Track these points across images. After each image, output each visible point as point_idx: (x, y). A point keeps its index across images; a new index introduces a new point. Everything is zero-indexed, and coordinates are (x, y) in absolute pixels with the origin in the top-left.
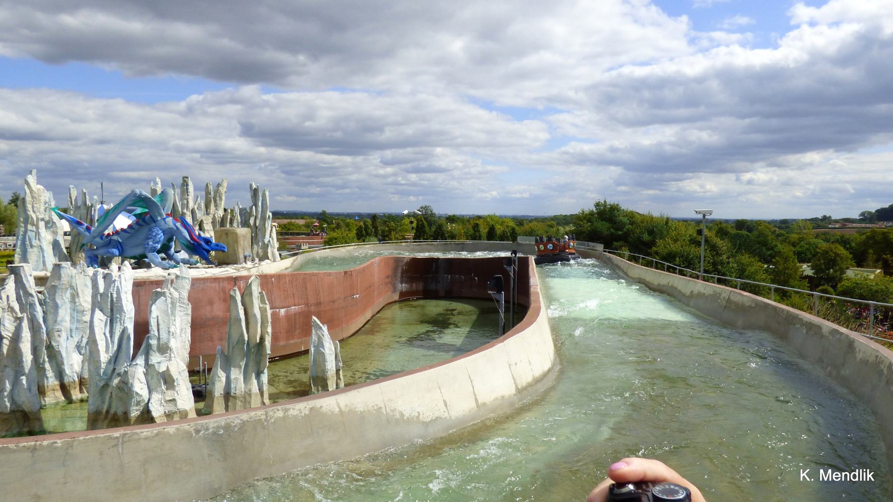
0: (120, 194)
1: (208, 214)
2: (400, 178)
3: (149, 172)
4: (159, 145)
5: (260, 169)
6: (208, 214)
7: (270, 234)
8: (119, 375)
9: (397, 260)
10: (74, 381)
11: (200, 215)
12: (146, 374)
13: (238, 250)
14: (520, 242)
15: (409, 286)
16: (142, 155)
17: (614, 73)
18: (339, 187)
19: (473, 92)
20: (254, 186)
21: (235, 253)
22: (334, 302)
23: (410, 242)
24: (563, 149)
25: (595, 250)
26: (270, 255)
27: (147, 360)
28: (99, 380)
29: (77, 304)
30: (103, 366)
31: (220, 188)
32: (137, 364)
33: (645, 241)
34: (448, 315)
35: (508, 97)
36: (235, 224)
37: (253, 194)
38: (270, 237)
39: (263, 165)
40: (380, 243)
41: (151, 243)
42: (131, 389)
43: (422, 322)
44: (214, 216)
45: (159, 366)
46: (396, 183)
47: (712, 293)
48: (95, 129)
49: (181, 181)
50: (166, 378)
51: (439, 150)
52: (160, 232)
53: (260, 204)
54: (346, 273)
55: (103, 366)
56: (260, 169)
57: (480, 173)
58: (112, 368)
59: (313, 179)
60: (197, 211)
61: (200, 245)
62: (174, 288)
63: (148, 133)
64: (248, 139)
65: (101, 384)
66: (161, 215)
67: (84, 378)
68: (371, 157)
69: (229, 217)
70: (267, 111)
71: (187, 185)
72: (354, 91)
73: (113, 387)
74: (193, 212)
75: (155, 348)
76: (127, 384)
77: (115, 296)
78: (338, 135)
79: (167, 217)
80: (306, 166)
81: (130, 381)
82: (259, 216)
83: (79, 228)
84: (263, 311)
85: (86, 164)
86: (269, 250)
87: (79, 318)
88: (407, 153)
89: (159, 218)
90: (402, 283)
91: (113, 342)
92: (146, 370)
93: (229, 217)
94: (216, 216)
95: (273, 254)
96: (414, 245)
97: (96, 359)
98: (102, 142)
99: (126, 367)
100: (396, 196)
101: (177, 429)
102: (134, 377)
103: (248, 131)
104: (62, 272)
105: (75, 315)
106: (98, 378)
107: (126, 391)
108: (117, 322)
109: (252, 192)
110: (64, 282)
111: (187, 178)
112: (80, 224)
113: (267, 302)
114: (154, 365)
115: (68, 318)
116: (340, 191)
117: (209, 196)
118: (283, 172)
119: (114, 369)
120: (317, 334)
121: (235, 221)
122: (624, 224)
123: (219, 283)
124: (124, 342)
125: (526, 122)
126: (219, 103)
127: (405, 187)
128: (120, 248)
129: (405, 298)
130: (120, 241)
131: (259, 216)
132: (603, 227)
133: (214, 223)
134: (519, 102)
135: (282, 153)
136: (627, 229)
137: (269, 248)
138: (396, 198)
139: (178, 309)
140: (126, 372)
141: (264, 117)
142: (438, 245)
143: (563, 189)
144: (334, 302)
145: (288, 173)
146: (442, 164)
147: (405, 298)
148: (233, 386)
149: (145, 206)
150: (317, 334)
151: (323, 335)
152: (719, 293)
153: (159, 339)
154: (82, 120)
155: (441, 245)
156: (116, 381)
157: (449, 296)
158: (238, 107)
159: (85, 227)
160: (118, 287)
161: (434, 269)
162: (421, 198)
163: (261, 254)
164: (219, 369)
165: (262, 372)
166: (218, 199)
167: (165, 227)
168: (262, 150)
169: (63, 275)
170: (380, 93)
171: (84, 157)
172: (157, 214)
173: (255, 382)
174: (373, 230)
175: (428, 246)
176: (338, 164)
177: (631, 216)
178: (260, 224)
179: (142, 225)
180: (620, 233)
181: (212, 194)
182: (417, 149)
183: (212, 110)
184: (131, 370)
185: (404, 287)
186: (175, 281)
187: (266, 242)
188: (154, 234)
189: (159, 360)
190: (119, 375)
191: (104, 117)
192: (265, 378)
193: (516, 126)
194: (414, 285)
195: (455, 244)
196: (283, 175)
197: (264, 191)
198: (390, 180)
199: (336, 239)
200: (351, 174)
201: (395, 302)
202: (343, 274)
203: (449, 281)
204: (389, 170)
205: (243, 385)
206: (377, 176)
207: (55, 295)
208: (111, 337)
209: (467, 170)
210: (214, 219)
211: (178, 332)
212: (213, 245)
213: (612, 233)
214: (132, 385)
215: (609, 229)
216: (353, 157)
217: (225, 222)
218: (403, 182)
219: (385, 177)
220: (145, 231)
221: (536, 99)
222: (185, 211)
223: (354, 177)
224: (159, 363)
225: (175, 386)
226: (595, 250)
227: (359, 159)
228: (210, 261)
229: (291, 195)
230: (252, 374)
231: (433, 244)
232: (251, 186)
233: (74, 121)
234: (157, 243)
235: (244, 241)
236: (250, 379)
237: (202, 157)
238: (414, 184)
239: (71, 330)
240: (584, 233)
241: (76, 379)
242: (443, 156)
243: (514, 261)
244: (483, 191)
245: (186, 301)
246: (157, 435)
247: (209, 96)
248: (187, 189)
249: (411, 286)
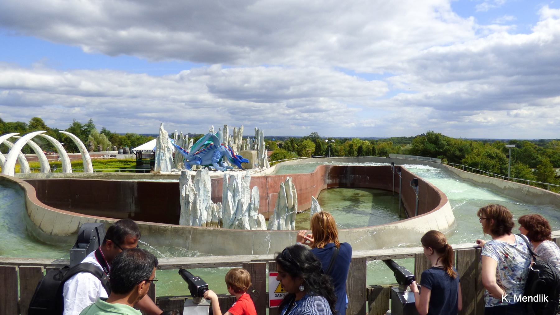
0: (141, 125)
1: (235, 143)
2: (297, 115)
3: (157, 114)
6: (235, 143)
7: (265, 153)
8: (238, 220)
9: (327, 167)
10: (205, 223)
11: (232, 144)
12: (249, 220)
13: (252, 162)
14: (391, 157)
15: (332, 181)
17: (425, 51)
18: (261, 121)
19: (342, 65)
20: (257, 129)
21: (251, 164)
22: (307, 189)
23: (329, 157)
24: (395, 97)
25: (436, 162)
26: (265, 164)
27: (249, 214)
28: (229, 222)
29: (206, 188)
30: (232, 216)
31: (240, 130)
32: (246, 216)
33: (457, 156)
34: (356, 196)
35: (363, 67)
36: (248, 149)
37: (256, 133)
38: (265, 155)
39: (218, 108)
40: (312, 158)
41: (215, 159)
42: (244, 227)
43: (345, 200)
44: (238, 144)
45: (254, 217)
46: (294, 119)
47: (518, 187)
48: (131, 90)
49: (223, 127)
50: (258, 222)
51: (321, 99)
52: (219, 153)
53: (260, 138)
54: (311, 174)
55: (232, 216)
56: (218, 111)
57: (345, 112)
58: (235, 217)
60: (231, 142)
61: (237, 159)
62: (244, 182)
65: (230, 224)
66: (219, 145)
67: (208, 222)
68: (282, 104)
69: (245, 145)
70: (223, 78)
71: (226, 129)
72: (274, 66)
73: (235, 225)
74: (229, 142)
75: (252, 208)
76: (241, 224)
77: (236, 185)
79: (222, 146)
80: (243, 109)
81: (244, 223)
83: (181, 151)
84: (294, 193)
87: (207, 195)
88: (302, 101)
89: (218, 146)
90: (328, 179)
91: (235, 206)
92: (249, 218)
93: (245, 145)
94: (239, 144)
95: (267, 164)
96: (331, 158)
97: (229, 213)
99: (241, 217)
100: (294, 126)
101: (362, 230)
102: (245, 221)
103: (213, 90)
104: (201, 174)
105: (205, 193)
106: (229, 221)
107: (241, 227)
108: (236, 197)
109: (256, 132)
110: (202, 178)
111: (226, 125)
112: (181, 149)
113: (295, 189)
114: (252, 216)
115: (203, 194)
116: (261, 124)
117: (236, 134)
119: (236, 217)
120: (314, 204)
121: (248, 147)
122: (444, 145)
123: (260, 179)
124: (240, 206)
125: (374, 81)
127: (300, 121)
128: (200, 161)
129: (330, 187)
130: (200, 157)
131: (259, 144)
132: (431, 147)
133: (238, 148)
134: (369, 70)
136: (446, 148)
137: (264, 160)
138: (293, 128)
139: (246, 191)
140: (241, 219)
142: (344, 158)
143: (395, 121)
144: (307, 189)
145: (232, 113)
146: (324, 107)
147: (330, 187)
148: (281, 227)
149: (212, 140)
150: (314, 204)
151: (317, 205)
152: (522, 188)
153: (254, 204)
154: (124, 85)
155: (346, 158)
156: (237, 223)
157: (352, 186)
159: (183, 150)
160: (237, 181)
161: (345, 171)
162: (309, 127)
163: (260, 164)
164: (275, 219)
165: (293, 221)
166: (239, 135)
167: (221, 151)
169: (202, 175)
172: (218, 144)
173: (290, 225)
174: (292, 148)
175: (340, 159)
176: (262, 108)
177: (449, 141)
178: (260, 148)
179: (210, 150)
180: (441, 150)
181: (237, 133)
182: (308, 99)
183: (194, 79)
184: (243, 218)
185: (329, 181)
186: (244, 178)
187: (263, 158)
188: (217, 154)
189: (254, 214)
190: (238, 220)
192: (294, 224)
193: (366, 84)
194: (334, 180)
195: (354, 158)
196: (230, 114)
197: (262, 131)
198: (291, 116)
199: (278, 154)
200: (269, 114)
201: (325, 189)
202: (310, 175)
203: (353, 178)
204: (292, 111)
205: (285, 227)
206: (284, 114)
207: (198, 184)
208: (234, 203)
209: (337, 111)
211: (245, 202)
212: (243, 160)
213: (436, 151)
214: (244, 224)
215: (434, 148)
216: (271, 104)
217: (243, 147)
218: (298, 118)
219: (288, 115)
220: (212, 153)
221: (379, 68)
222: (225, 142)
223: (270, 115)
224: (254, 215)
225: (261, 226)
226: (436, 162)
227: (274, 105)
228: (241, 168)
230: (289, 222)
231: (341, 158)
232: (255, 129)
233: (120, 86)
234: (218, 158)
235: (255, 157)
236: (288, 224)
238: (306, 119)
239: (204, 200)
240: (419, 150)
241: (206, 222)
242: (324, 103)
243: (393, 168)
244: (346, 123)
245: (249, 188)
246: (358, 231)
248: (226, 131)
249: (333, 181)
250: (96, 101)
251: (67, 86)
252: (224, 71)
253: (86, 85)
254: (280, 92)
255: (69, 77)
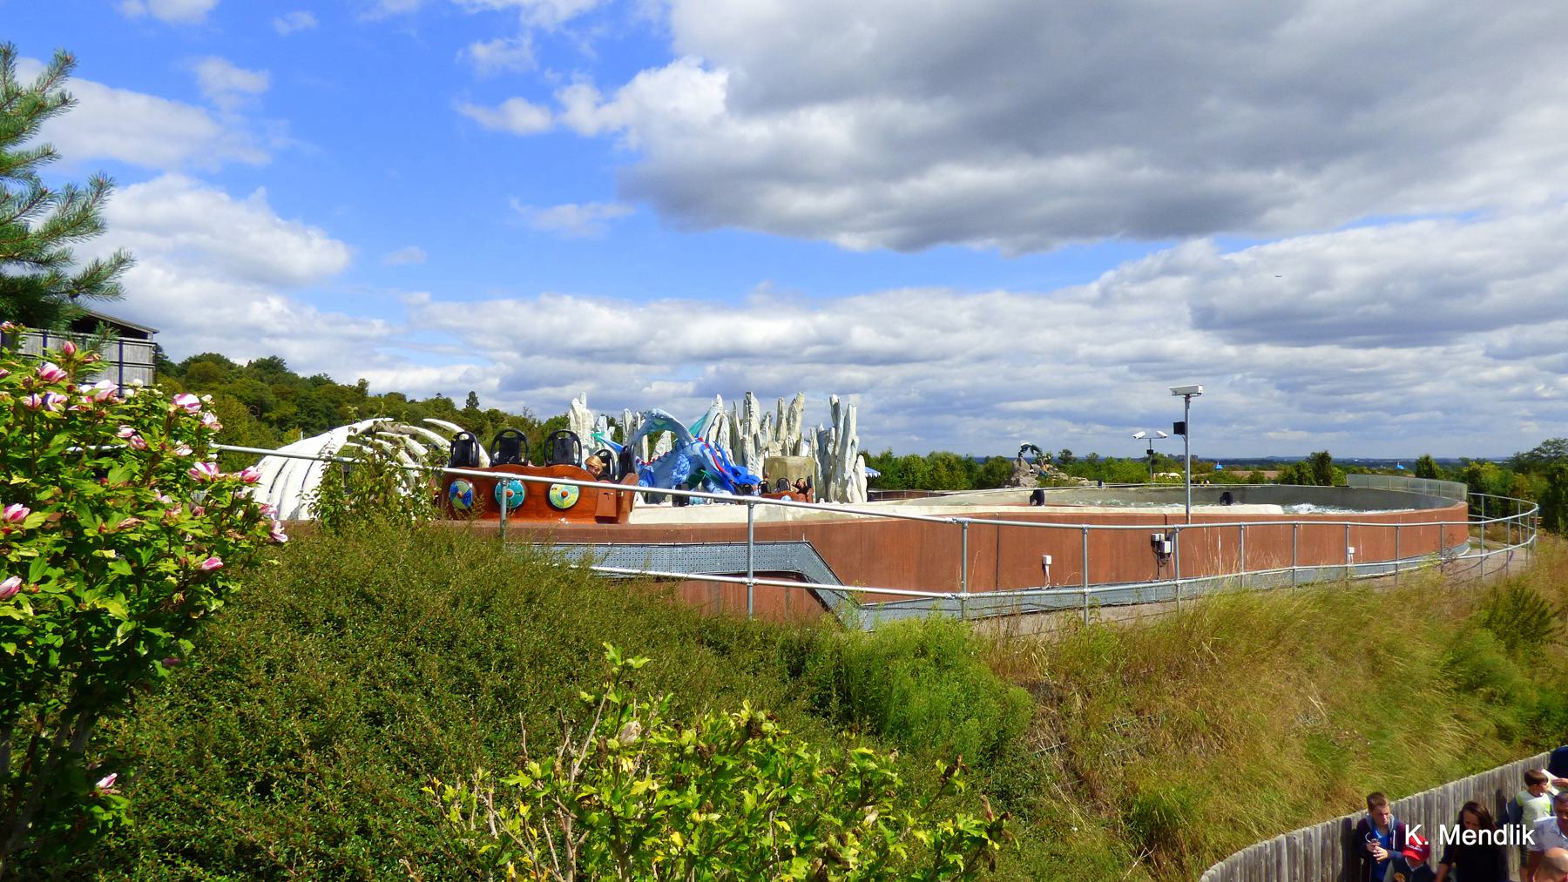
4: (1063, 356)
5: (1232, 385)
16: (1044, 373)
18: (1394, 411)
39: (1238, 377)
59: (1337, 398)
63: (1048, 338)
64: (1209, 333)
70: (1235, 282)
78: (1383, 309)
82: (840, 441)
85: (962, 394)
86: (848, 490)
98: (983, 358)
103: (1206, 320)
116: (1397, 419)
118: (1281, 387)
126: (1145, 278)
135: (1269, 353)
141: (1232, 292)
145: (1292, 388)
154: (954, 329)
158: (1185, 279)
168: (1230, 351)
170: (1468, 217)
171: (960, 383)
183: (1138, 290)
191: (984, 320)
196: (1277, 393)
200: (1418, 383)
210: (784, 446)
223: (1424, 389)
229: (1295, 428)
237: (1131, 370)
247: (1128, 269)
250: (893, 374)
251: (818, 343)
252: (1241, 258)
253: (863, 337)
254: (1456, 306)
255: (824, 321)
